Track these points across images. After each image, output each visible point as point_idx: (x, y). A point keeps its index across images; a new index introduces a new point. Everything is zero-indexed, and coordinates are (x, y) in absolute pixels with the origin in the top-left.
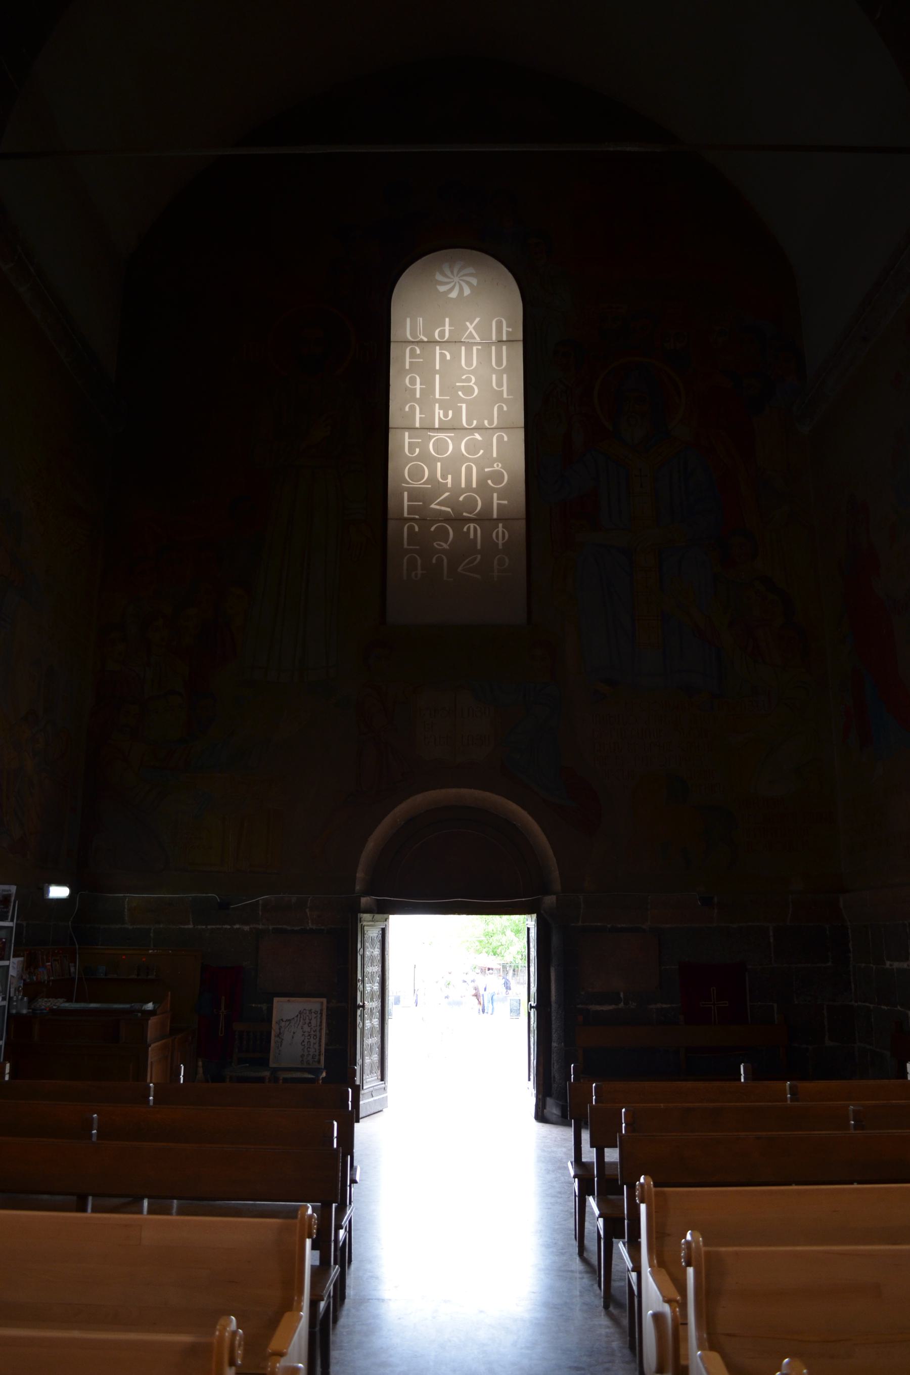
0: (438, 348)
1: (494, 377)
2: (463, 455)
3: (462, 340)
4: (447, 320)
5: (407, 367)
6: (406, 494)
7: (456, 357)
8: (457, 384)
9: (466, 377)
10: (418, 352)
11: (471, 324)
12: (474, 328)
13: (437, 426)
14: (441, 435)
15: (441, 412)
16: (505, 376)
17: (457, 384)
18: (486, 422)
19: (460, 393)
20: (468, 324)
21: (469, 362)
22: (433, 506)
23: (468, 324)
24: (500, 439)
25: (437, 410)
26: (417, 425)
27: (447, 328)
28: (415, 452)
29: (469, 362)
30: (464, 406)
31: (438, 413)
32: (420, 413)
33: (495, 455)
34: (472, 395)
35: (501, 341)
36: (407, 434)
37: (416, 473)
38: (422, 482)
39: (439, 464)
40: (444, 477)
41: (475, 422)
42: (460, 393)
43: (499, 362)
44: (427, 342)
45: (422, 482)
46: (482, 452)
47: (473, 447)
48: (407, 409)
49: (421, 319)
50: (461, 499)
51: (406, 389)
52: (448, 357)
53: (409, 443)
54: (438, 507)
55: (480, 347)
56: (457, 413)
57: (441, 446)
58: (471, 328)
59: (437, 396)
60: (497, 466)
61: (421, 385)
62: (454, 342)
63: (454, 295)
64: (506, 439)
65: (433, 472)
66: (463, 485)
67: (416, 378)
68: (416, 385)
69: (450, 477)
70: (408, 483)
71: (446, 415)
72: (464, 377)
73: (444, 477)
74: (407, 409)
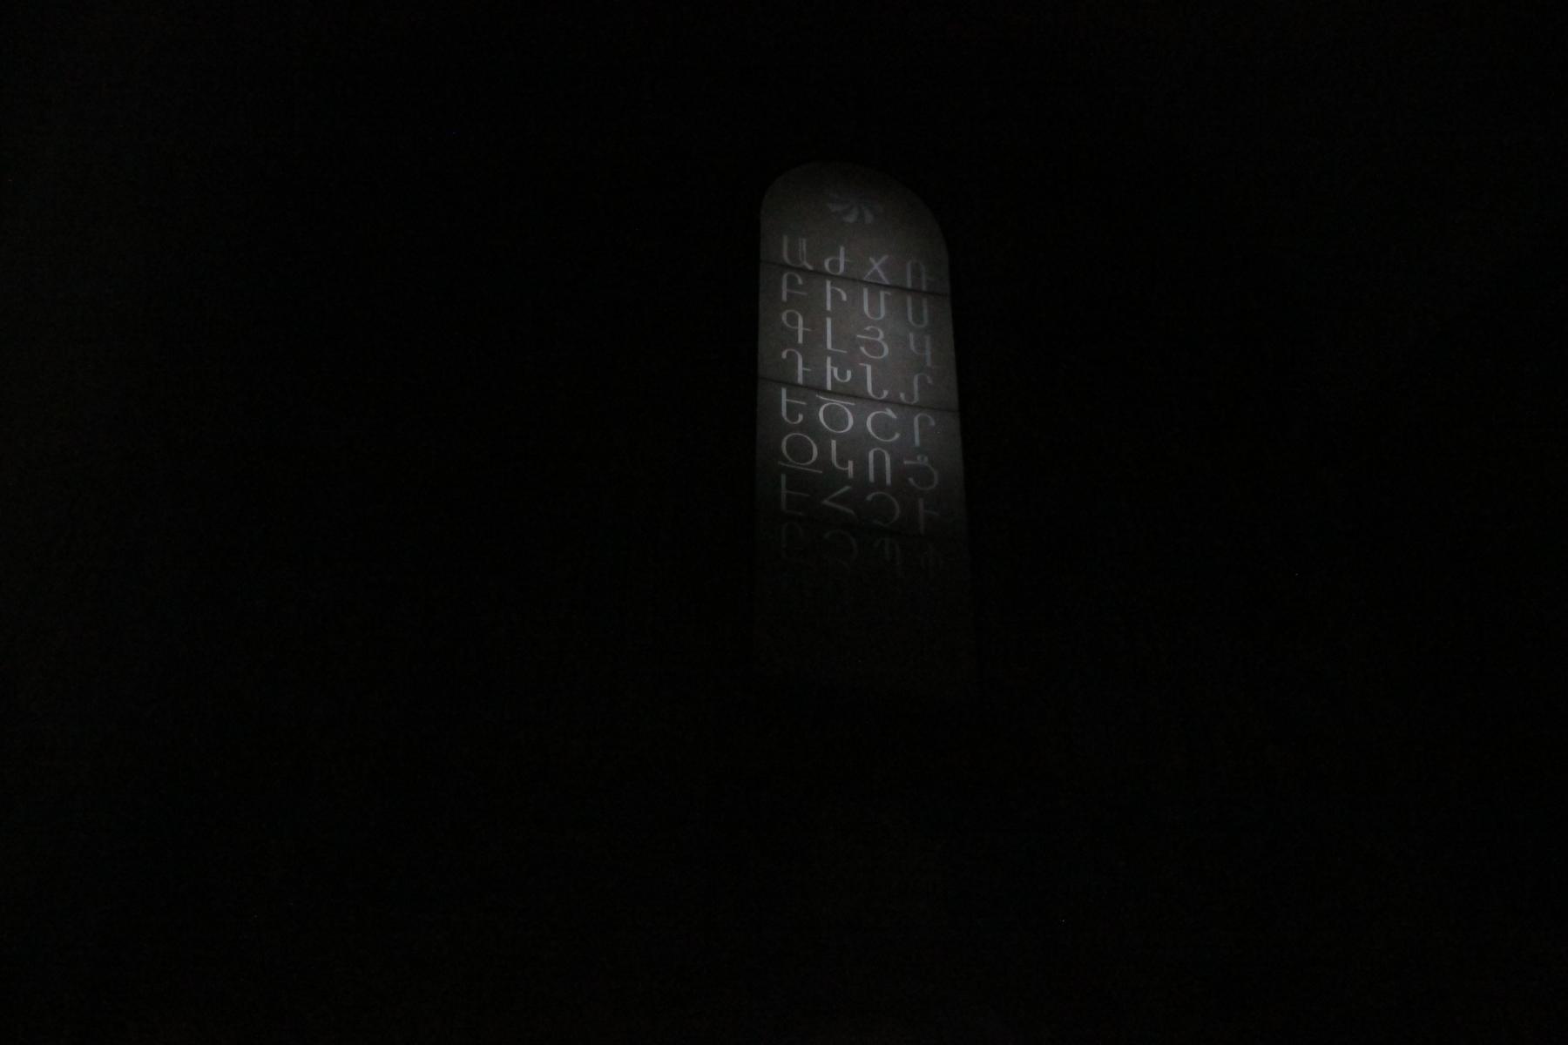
0: (828, 283)
1: (911, 336)
2: (869, 435)
3: (865, 279)
4: (842, 249)
5: (784, 298)
6: (783, 478)
7: (856, 299)
8: (859, 336)
9: (872, 329)
10: (800, 281)
11: (877, 261)
12: (881, 266)
13: (829, 387)
14: (837, 402)
15: (836, 370)
16: (928, 338)
17: (859, 336)
18: (902, 396)
19: (863, 349)
20: (872, 260)
21: (875, 311)
22: (826, 502)
23: (872, 260)
24: (923, 421)
25: (829, 367)
26: (800, 380)
27: (842, 260)
28: (797, 419)
29: (874, 309)
30: (869, 369)
31: (831, 371)
32: (805, 365)
33: (917, 441)
34: (881, 355)
35: (915, 291)
36: (784, 392)
37: (799, 450)
38: (808, 463)
39: (834, 443)
40: (843, 462)
41: (886, 393)
42: (863, 349)
43: (918, 317)
44: (811, 271)
45: (808, 463)
46: (897, 436)
47: (883, 426)
48: (784, 355)
49: (804, 240)
50: (869, 498)
51: (783, 328)
52: (844, 297)
53: (788, 404)
54: (833, 505)
55: (889, 293)
56: (859, 377)
57: (835, 417)
58: (876, 266)
59: (829, 346)
60: (921, 460)
61: (805, 326)
62: (851, 280)
63: (851, 219)
64: (933, 423)
65: (824, 451)
66: (872, 477)
67: (797, 317)
68: (797, 324)
69: (851, 464)
70: (786, 461)
71: (842, 374)
72: (868, 328)
73: (843, 462)
74: (784, 355)
